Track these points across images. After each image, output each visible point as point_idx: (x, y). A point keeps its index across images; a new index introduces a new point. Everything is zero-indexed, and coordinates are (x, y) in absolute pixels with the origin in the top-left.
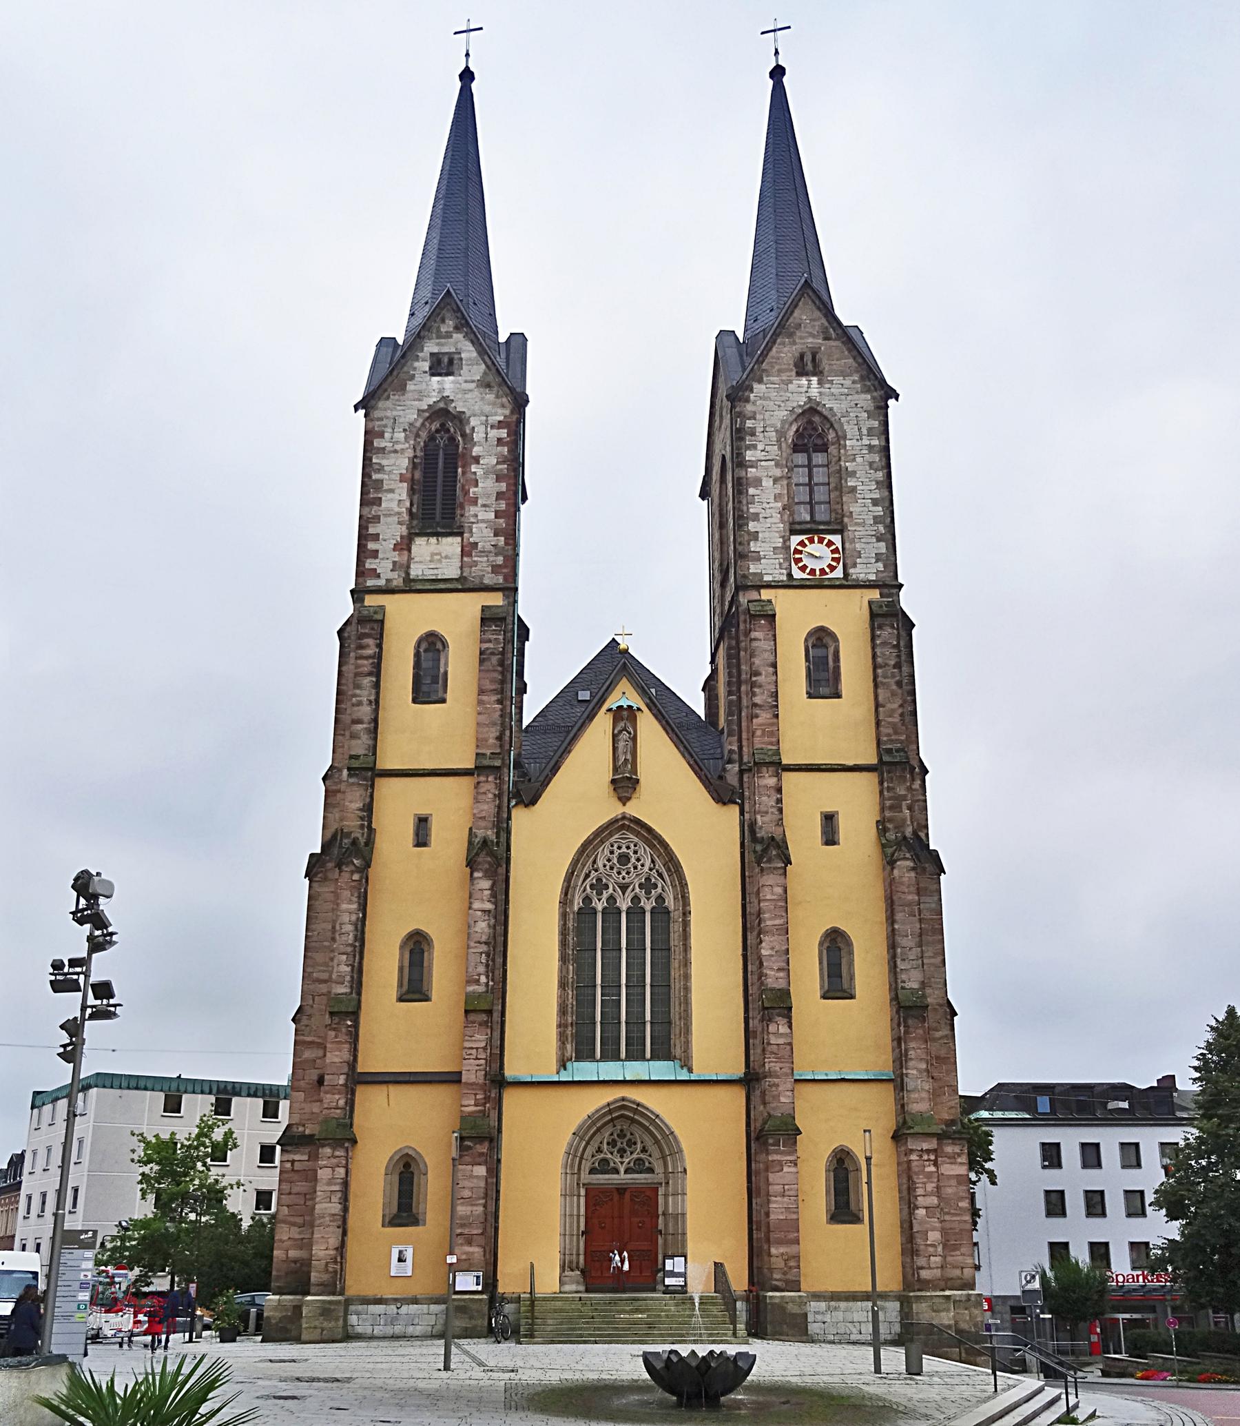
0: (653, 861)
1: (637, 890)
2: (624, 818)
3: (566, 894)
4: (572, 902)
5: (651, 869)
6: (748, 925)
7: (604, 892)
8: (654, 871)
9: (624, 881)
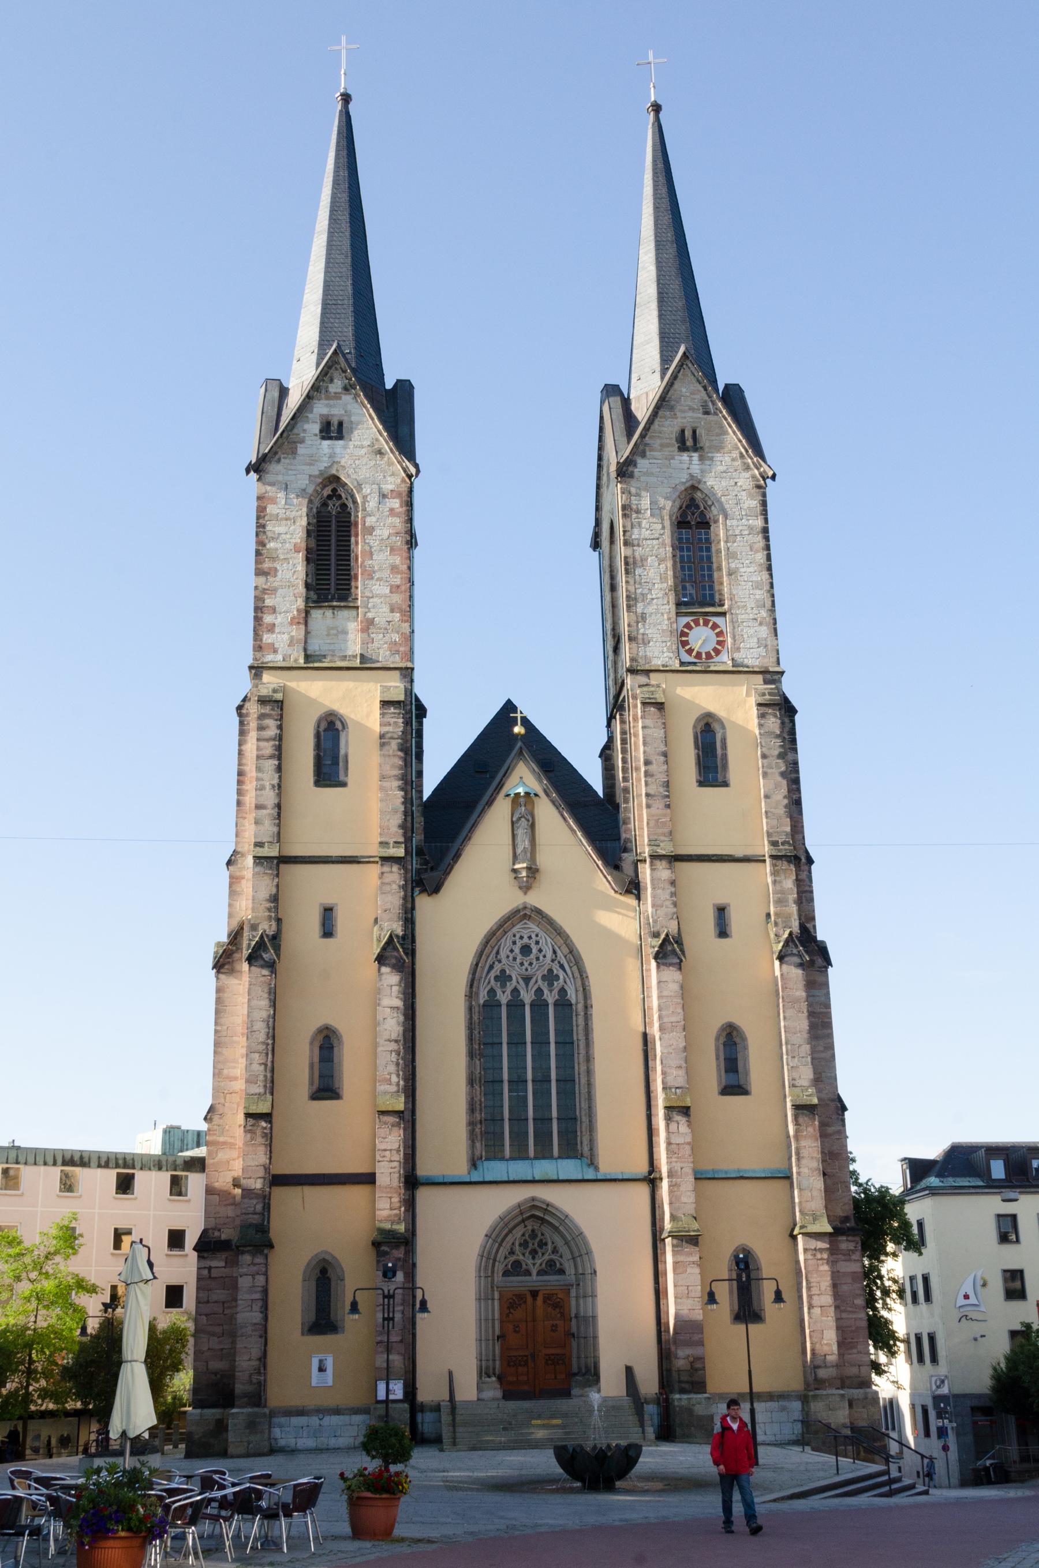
0: (555, 952)
1: (540, 982)
2: (525, 908)
3: (471, 986)
4: (477, 994)
5: (553, 961)
7: (508, 984)
8: (556, 962)
9: (527, 973)
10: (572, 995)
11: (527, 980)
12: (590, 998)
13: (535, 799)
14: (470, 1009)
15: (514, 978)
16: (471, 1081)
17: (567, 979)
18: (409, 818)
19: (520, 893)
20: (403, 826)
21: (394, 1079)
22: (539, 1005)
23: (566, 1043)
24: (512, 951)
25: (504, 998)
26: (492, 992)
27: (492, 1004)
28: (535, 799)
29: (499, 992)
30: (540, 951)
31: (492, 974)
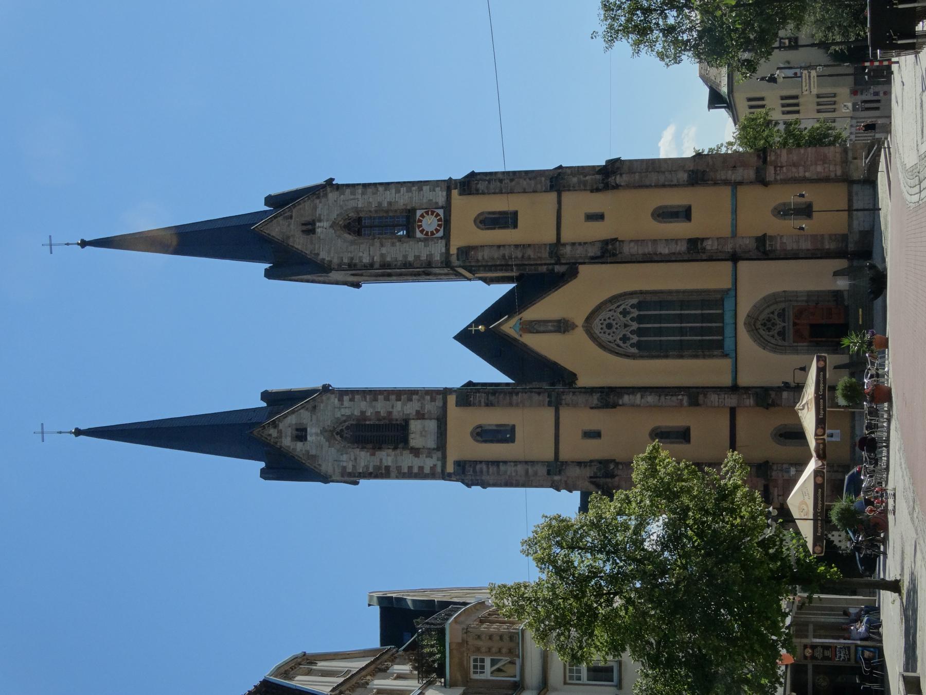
0: (610, 311)
4: (634, 353)
5: (615, 312)
6: (649, 260)
7: (627, 336)
10: (635, 301)
11: (626, 326)
12: (636, 291)
13: (523, 319)
14: (642, 357)
15: (624, 333)
16: (681, 357)
17: (626, 303)
18: (534, 390)
19: (577, 329)
20: (539, 394)
21: (680, 397)
22: (640, 319)
23: (661, 305)
24: (609, 334)
25: (635, 339)
26: (632, 345)
27: (638, 345)
28: (523, 319)
29: (632, 341)
30: (609, 318)
31: (622, 344)
